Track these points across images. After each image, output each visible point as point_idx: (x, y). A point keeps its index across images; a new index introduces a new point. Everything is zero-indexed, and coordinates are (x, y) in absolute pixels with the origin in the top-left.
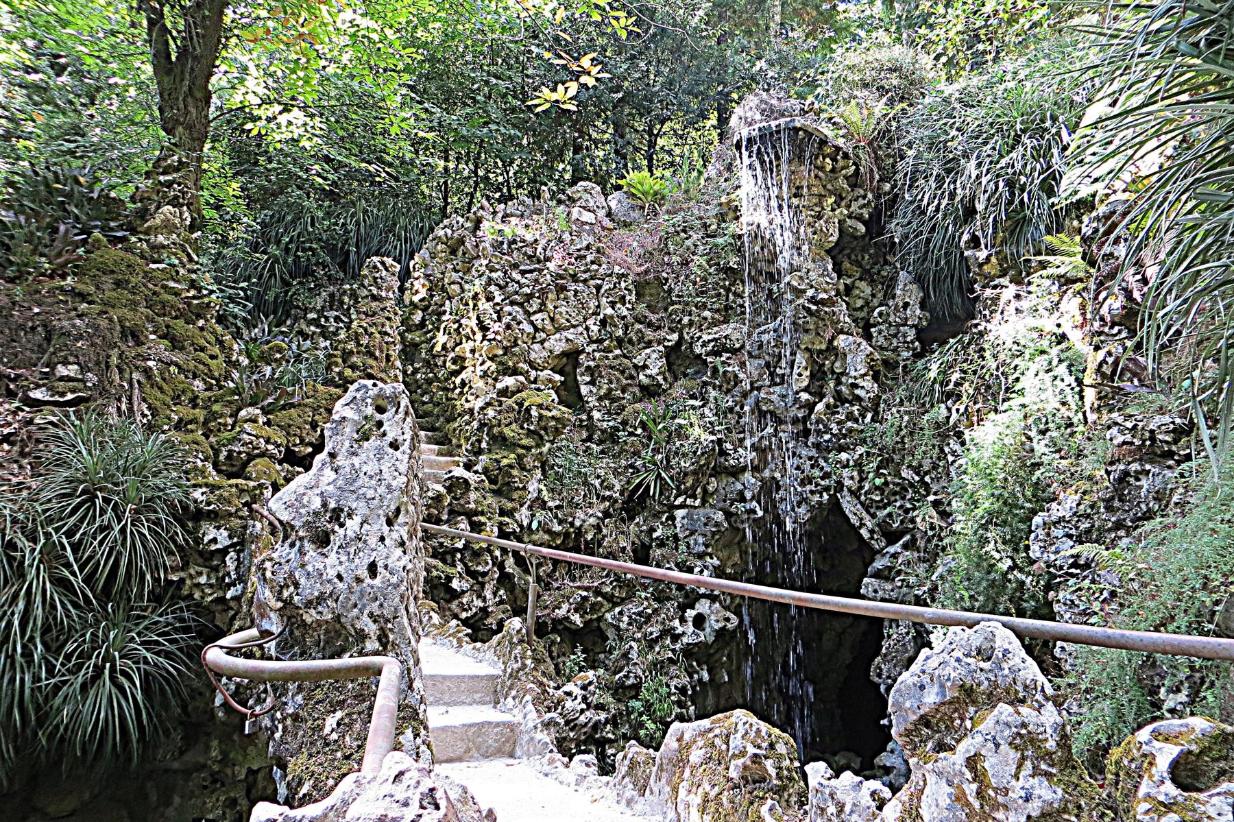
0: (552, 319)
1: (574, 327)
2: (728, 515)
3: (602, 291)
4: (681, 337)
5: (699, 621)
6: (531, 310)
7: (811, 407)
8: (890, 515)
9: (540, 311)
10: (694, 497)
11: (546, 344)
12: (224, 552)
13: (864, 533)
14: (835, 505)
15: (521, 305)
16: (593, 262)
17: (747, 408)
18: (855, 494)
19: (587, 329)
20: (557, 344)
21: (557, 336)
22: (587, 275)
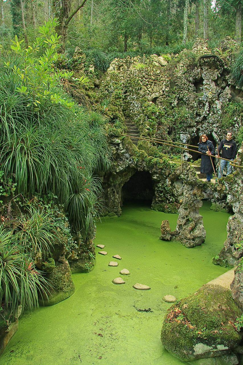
0: (153, 90)
1: (158, 92)
2: (190, 135)
3: (164, 84)
4: (179, 96)
5: (185, 156)
6: (148, 88)
7: (208, 114)
8: (222, 137)
9: (150, 88)
10: (184, 132)
11: (152, 96)
12: (120, 143)
13: (217, 140)
14: (211, 133)
15: (146, 86)
16: (161, 77)
17: (195, 113)
18: (216, 133)
19: (160, 93)
20: (154, 96)
21: (154, 94)
22: (160, 80)
